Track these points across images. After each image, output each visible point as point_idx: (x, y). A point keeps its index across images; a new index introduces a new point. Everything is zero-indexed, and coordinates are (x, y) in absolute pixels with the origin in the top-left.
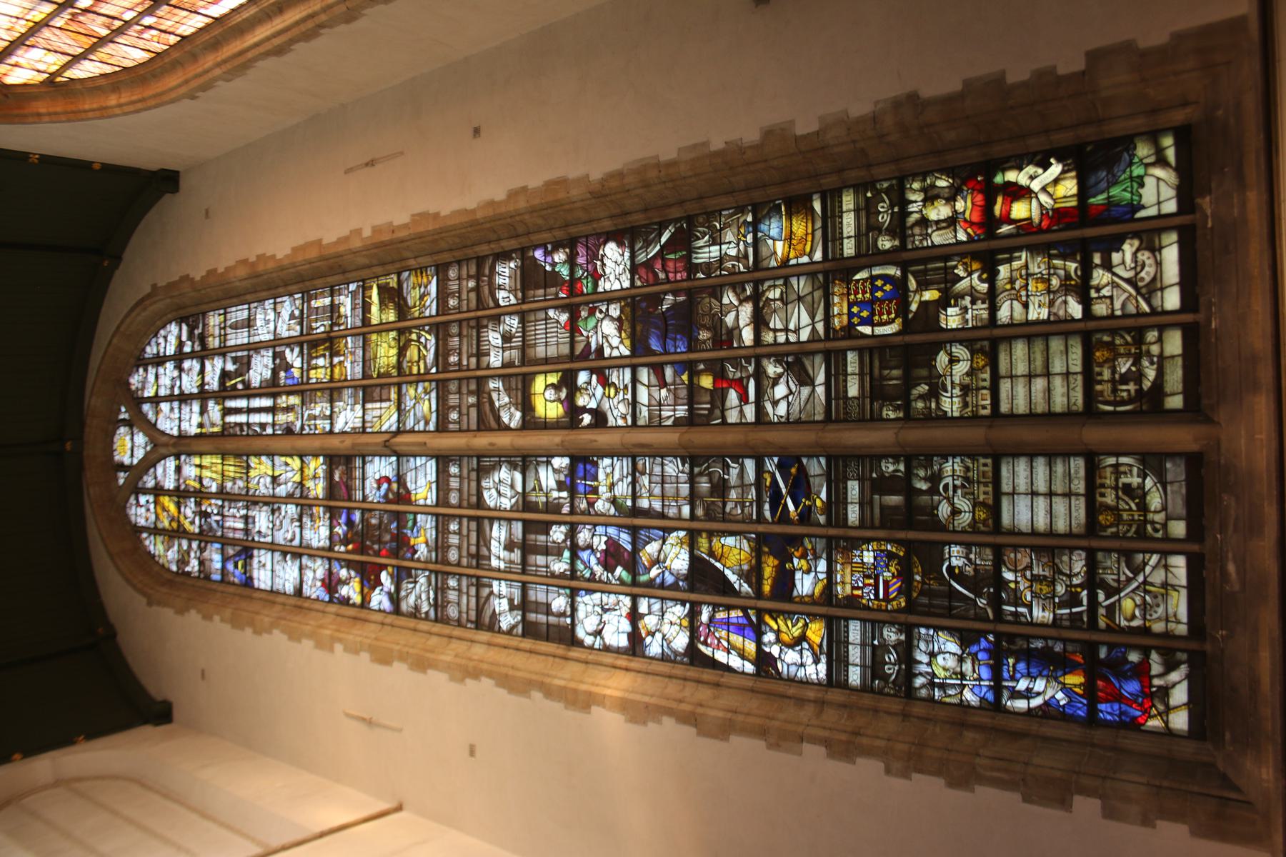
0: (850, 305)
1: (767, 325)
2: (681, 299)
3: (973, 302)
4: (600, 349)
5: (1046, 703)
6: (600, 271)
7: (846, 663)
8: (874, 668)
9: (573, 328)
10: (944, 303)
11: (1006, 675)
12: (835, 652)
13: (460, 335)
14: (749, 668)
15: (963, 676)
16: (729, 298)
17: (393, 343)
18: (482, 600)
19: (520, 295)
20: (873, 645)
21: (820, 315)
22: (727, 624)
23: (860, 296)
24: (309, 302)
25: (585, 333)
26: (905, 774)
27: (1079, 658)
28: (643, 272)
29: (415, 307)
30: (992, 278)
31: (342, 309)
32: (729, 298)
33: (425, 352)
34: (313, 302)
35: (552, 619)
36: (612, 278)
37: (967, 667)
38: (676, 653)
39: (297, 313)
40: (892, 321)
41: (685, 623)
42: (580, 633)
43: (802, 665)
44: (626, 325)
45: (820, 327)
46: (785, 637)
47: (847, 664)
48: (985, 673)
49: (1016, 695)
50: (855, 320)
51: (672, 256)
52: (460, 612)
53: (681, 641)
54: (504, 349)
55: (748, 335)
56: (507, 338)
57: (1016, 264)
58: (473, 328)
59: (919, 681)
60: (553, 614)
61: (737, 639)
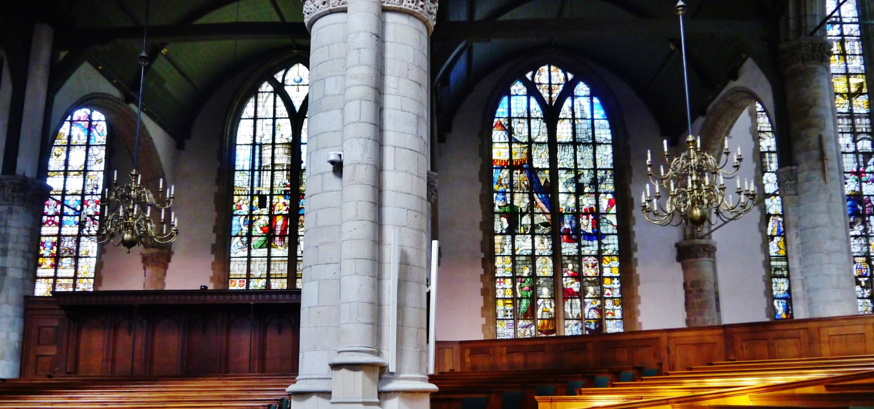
0: (861, 263)
1: (855, 239)
2: (861, 212)
3: (862, 294)
4: (846, 183)
5: (778, 310)
6: (868, 183)
7: (777, 260)
8: (777, 269)
9: (852, 173)
10: (862, 287)
11: (782, 300)
12: (778, 258)
13: (848, 124)
14: (769, 233)
15: (780, 291)
16: (862, 228)
17: (844, 90)
18: (767, 133)
19: (861, 151)
20: (782, 268)
21: (858, 254)
22: (779, 226)
23: (863, 265)
24: (857, 40)
25: (851, 178)
26: (764, 281)
27: (789, 317)
28: (868, 199)
29: (857, 102)
30: (867, 298)
31: (854, 61)
32: (862, 228)
33: (842, 107)
34: (856, 43)
35: (768, 163)
36: (866, 188)
37: (782, 292)
38: (768, 209)
39: (852, 33)
40: (857, 273)
41: (777, 213)
42: (766, 174)
43: (774, 249)
44: (853, 193)
45: (855, 254)
46: (779, 244)
47: (776, 261)
48: (782, 296)
49: (778, 302)
50: (857, 264)
51: (872, 209)
52: (762, 123)
53: (772, 211)
54: (845, 144)
55: (852, 233)
56: (848, 146)
57: (870, 304)
58: (851, 130)
59: (776, 279)
60: (770, 164)
61: (776, 229)
